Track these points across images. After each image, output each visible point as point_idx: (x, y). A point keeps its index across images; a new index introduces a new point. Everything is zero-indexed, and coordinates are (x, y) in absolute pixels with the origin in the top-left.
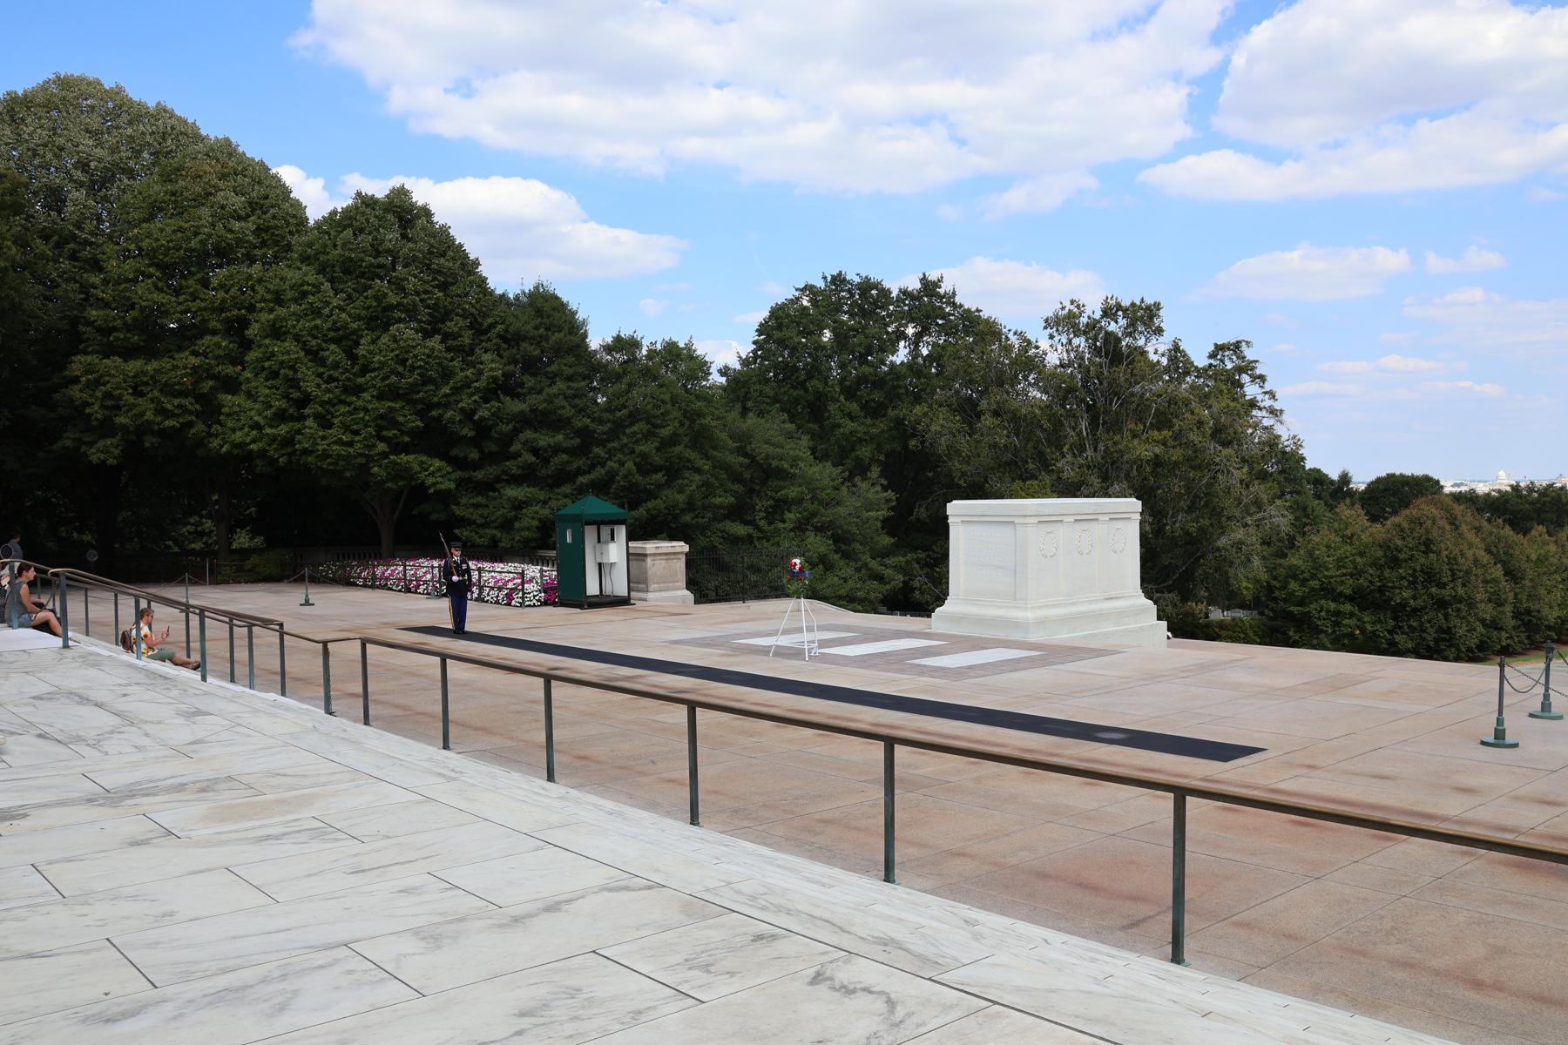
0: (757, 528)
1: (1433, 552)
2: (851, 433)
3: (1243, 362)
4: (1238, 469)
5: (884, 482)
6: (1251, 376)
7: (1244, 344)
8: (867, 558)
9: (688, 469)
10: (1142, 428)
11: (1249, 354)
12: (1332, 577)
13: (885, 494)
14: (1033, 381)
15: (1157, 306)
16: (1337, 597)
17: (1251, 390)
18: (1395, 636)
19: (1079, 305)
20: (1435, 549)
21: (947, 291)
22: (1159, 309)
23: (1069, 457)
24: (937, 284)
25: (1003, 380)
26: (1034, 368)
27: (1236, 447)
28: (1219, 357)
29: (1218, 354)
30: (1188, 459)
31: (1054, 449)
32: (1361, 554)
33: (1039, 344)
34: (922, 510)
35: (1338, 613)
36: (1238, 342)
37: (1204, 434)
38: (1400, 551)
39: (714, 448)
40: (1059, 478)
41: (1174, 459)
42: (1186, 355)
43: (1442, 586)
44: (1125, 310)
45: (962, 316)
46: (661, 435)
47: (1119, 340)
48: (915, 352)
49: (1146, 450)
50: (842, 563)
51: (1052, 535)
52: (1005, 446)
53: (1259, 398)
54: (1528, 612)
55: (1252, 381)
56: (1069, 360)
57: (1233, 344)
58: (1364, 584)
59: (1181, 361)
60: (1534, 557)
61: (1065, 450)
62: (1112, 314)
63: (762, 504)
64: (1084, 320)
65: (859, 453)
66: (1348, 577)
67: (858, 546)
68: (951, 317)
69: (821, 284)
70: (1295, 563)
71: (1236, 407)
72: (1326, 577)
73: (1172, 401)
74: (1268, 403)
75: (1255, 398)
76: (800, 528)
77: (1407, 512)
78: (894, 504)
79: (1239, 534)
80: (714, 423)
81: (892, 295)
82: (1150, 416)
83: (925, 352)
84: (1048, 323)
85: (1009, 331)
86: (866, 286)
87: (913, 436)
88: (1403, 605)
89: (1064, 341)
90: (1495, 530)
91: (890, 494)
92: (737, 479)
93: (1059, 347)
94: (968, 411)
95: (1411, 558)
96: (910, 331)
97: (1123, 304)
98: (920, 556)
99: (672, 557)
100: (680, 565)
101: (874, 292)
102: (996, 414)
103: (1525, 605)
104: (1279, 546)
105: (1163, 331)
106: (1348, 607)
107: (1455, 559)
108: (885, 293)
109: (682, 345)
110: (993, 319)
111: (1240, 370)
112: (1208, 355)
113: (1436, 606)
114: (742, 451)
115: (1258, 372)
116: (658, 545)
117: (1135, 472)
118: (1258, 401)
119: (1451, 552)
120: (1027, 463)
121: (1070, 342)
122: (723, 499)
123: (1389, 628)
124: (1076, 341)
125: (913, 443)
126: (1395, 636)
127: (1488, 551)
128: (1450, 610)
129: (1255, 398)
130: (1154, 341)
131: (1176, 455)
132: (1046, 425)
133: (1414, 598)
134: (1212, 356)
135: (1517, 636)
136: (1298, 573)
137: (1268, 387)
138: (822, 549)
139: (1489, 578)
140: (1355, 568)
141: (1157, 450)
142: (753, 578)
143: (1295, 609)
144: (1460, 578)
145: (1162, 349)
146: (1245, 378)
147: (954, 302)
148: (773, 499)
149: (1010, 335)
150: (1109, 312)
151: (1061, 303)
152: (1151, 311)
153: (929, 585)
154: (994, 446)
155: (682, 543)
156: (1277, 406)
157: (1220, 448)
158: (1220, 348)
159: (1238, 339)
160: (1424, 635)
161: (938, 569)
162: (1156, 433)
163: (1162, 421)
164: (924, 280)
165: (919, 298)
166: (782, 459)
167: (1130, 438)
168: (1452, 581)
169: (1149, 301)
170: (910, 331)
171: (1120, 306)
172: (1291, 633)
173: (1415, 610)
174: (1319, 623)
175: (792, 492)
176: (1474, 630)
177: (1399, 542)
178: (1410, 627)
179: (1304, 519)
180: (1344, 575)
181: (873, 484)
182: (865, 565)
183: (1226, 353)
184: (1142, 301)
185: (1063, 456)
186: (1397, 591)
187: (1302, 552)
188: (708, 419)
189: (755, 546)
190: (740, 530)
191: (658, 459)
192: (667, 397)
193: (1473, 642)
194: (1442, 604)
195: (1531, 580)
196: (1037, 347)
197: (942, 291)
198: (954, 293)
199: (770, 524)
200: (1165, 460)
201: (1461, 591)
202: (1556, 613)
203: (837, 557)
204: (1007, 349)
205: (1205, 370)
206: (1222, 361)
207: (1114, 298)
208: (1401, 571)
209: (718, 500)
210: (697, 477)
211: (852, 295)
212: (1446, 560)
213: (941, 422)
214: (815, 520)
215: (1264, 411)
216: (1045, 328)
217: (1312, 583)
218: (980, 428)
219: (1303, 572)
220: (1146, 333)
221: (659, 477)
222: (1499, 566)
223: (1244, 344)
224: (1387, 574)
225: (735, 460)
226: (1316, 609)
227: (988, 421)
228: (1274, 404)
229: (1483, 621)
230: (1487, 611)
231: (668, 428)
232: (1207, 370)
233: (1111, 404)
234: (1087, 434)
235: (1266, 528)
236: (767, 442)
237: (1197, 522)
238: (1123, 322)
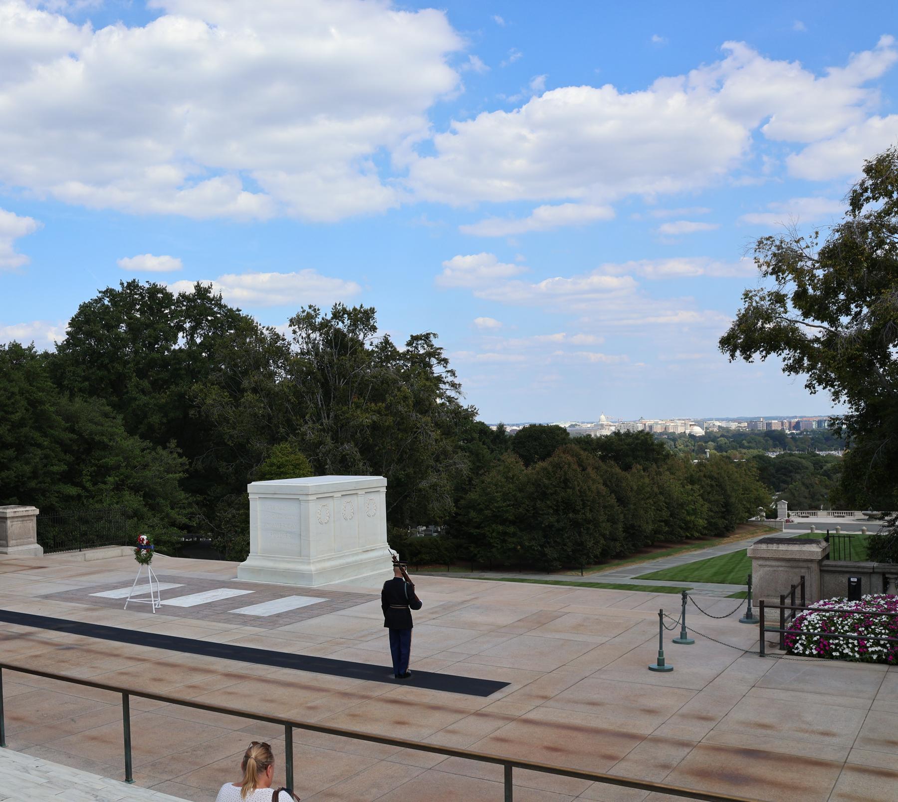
0: (84, 488)
1: (570, 488)
2: (144, 405)
3: (432, 349)
4: (433, 431)
5: (180, 451)
6: (437, 359)
7: (432, 335)
8: (168, 509)
9: (32, 445)
10: (363, 401)
11: (436, 343)
12: (499, 507)
13: (180, 460)
14: (280, 365)
15: (372, 311)
16: (504, 522)
17: (438, 370)
18: (545, 549)
19: (315, 309)
20: (571, 485)
21: (216, 296)
22: (373, 313)
23: (310, 424)
24: (207, 290)
25: (260, 362)
26: (282, 355)
27: (431, 415)
28: (414, 345)
29: (413, 343)
30: (399, 424)
31: (298, 417)
32: (521, 490)
33: (285, 337)
34: (199, 463)
35: (505, 533)
36: (428, 334)
37: (407, 405)
39: (51, 427)
40: (303, 440)
41: (387, 424)
42: (393, 346)
43: (575, 512)
44: (349, 314)
45: (226, 314)
46: (12, 420)
47: (345, 335)
48: (191, 342)
49: (366, 418)
50: (150, 514)
51: (326, 507)
52: (263, 416)
53: (444, 375)
54: (633, 526)
55: (438, 363)
56: (308, 350)
57: (424, 335)
58: (523, 512)
59: (390, 351)
60: (635, 488)
61: (307, 418)
62: (340, 316)
63: (87, 470)
64: (318, 320)
65: (150, 420)
66: (512, 507)
67: (162, 501)
68: (219, 315)
69: (119, 289)
70: (473, 497)
71: (430, 385)
72: (496, 508)
73: (385, 381)
74: (450, 379)
75: (441, 375)
76: (118, 487)
77: (551, 459)
78: (187, 467)
79: (433, 478)
80: (52, 409)
81: (173, 298)
82: (367, 391)
83: (198, 341)
84: (292, 322)
85: (264, 327)
86: (154, 290)
87: (192, 407)
88: (550, 526)
89: (304, 335)
90: (609, 469)
91: (184, 459)
92: (66, 449)
93: (300, 340)
94: (233, 386)
95: (555, 493)
96: (187, 325)
97: (348, 309)
98: (199, 499)
99: (27, 518)
100: (32, 525)
101: (160, 295)
102: (255, 391)
103: (631, 522)
104: (461, 488)
105: (376, 329)
106: (511, 529)
108: (168, 296)
109: (24, 346)
110: (249, 317)
111: (430, 355)
112: (406, 343)
113: (573, 527)
114: (72, 430)
115: (443, 356)
116: (15, 510)
117: (358, 434)
118: (443, 378)
119: (582, 488)
120: (279, 427)
121: (308, 336)
122: (59, 468)
124: (313, 336)
125: (192, 412)
126: (545, 549)
127: (605, 484)
128: (582, 529)
129: (441, 375)
130: (370, 336)
131: (389, 421)
132: (293, 399)
133: (558, 521)
134: (409, 344)
135: (627, 544)
136: (476, 504)
137: (449, 367)
138: (135, 505)
139: (607, 504)
140: (516, 500)
141: (374, 418)
142: (84, 528)
143: (475, 531)
144: (589, 506)
145: (376, 342)
146: (434, 361)
147: (220, 303)
148: (96, 465)
149: (264, 331)
150: (338, 314)
151: (302, 308)
152: (368, 314)
153: (206, 521)
154: (255, 415)
155: (34, 508)
156: (456, 381)
157: (419, 416)
158: (415, 338)
159: (428, 332)
161: (218, 514)
162: (373, 405)
163: (378, 395)
164: (198, 287)
165: (194, 300)
166: (103, 435)
167: (354, 408)
168: (583, 508)
169: (367, 307)
170: (187, 325)
171: (346, 310)
172: (472, 549)
174: (491, 541)
175: (111, 461)
176: (598, 542)
177: (546, 482)
179: (479, 466)
180: (509, 506)
181: (171, 452)
182: (168, 515)
183: (420, 342)
184: (361, 307)
185: (306, 423)
186: (547, 516)
187: (478, 489)
188: (47, 406)
189: (83, 503)
190: (73, 491)
191: (9, 439)
192: (16, 390)
193: (598, 552)
194: (576, 524)
195: (635, 504)
196: (284, 340)
197: (211, 295)
198: (221, 297)
199: (95, 484)
200: (380, 425)
201: (589, 515)
202: (651, 527)
203: (145, 509)
204: (261, 340)
205: (405, 354)
206: (416, 348)
207: (341, 304)
208: (548, 502)
209: (55, 469)
210: (39, 452)
211: (143, 298)
212: (578, 493)
213: (214, 397)
214: (129, 481)
215: (447, 384)
216: (290, 326)
217: (487, 512)
218: (244, 402)
219: (479, 504)
220: (364, 330)
221: (11, 452)
222: (613, 495)
223: (432, 335)
224: (539, 504)
225: (67, 436)
226: (489, 531)
227: (249, 396)
228: (454, 380)
229: (604, 536)
230: (606, 528)
231: (18, 414)
232: (406, 355)
233: (339, 383)
234: (322, 404)
235: (453, 472)
236: (91, 421)
237: (404, 471)
238: (347, 322)
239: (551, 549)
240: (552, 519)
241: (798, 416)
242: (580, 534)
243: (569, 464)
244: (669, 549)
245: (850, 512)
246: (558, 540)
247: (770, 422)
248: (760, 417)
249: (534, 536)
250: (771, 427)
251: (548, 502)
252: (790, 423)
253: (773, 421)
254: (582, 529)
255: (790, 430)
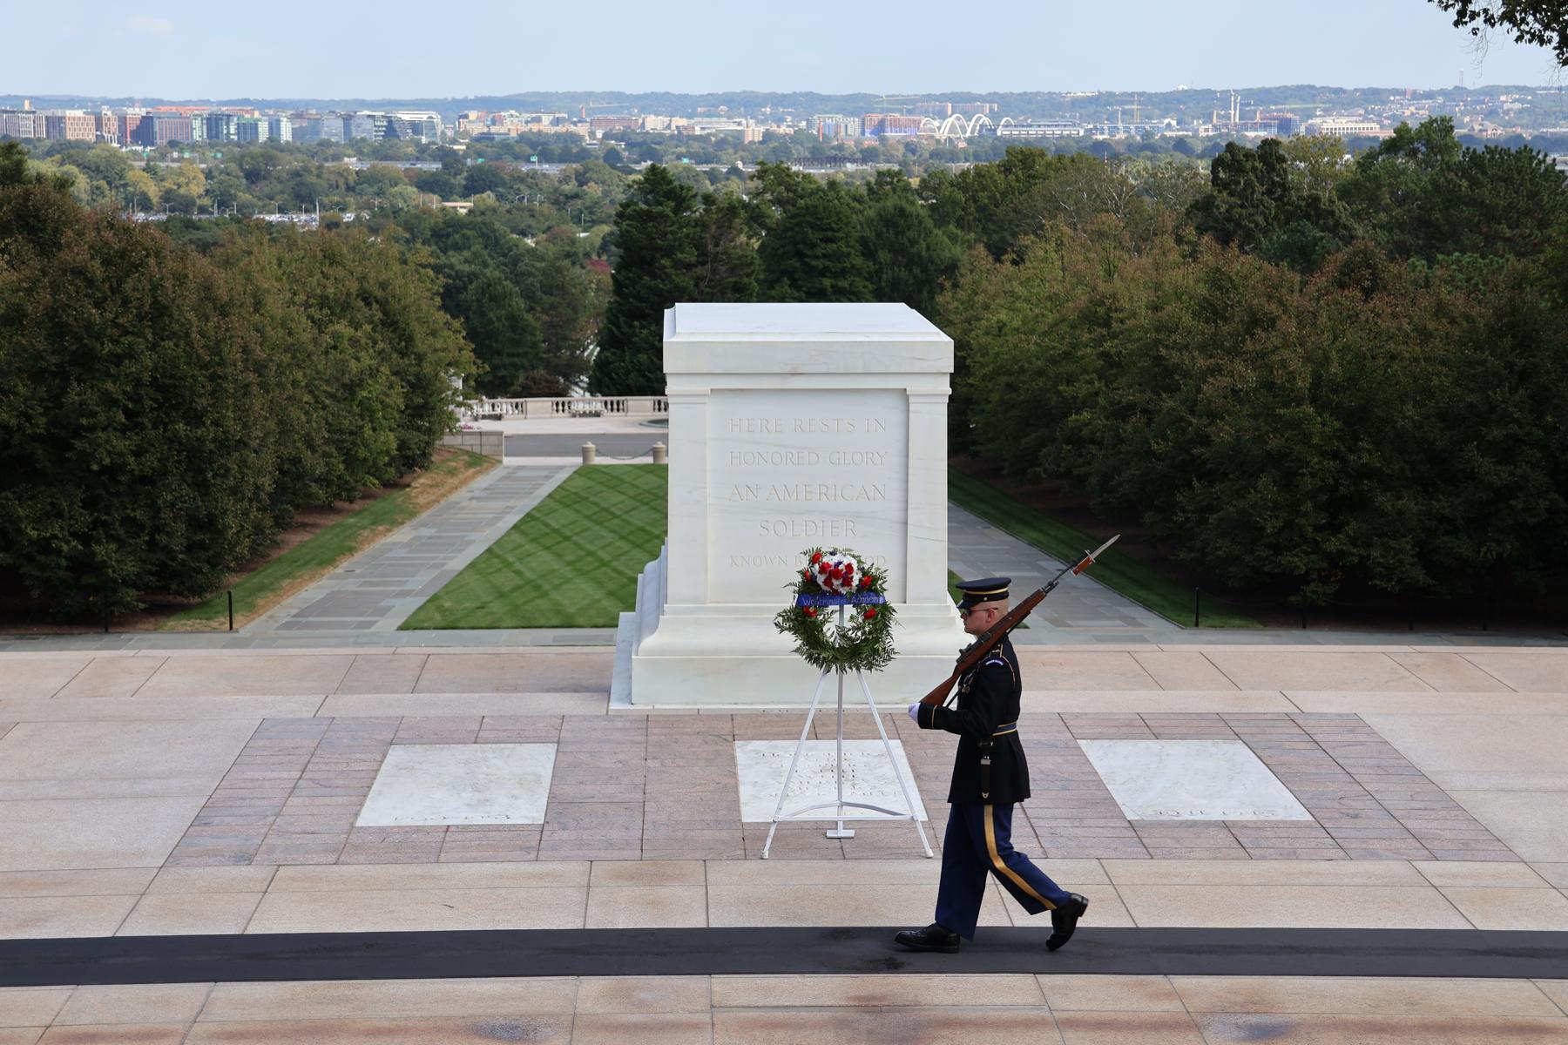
38: (99, 337)
43: (196, 418)
88: (112, 471)
107: (219, 353)
123: (78, 528)
128: (210, 475)
133: (137, 453)
160: (162, 539)
173: (145, 480)
178: (128, 521)
208: (109, 385)
239: (113, 546)
240: (121, 444)
241: (136, 97)
242: (202, 487)
243: (157, 254)
244: (318, 531)
245: (615, 399)
246: (138, 514)
247: (60, 115)
248: (23, 98)
249: (52, 504)
250: (62, 131)
251: (109, 385)
252: (123, 120)
253: (69, 113)
254: (210, 475)
255: (122, 142)
